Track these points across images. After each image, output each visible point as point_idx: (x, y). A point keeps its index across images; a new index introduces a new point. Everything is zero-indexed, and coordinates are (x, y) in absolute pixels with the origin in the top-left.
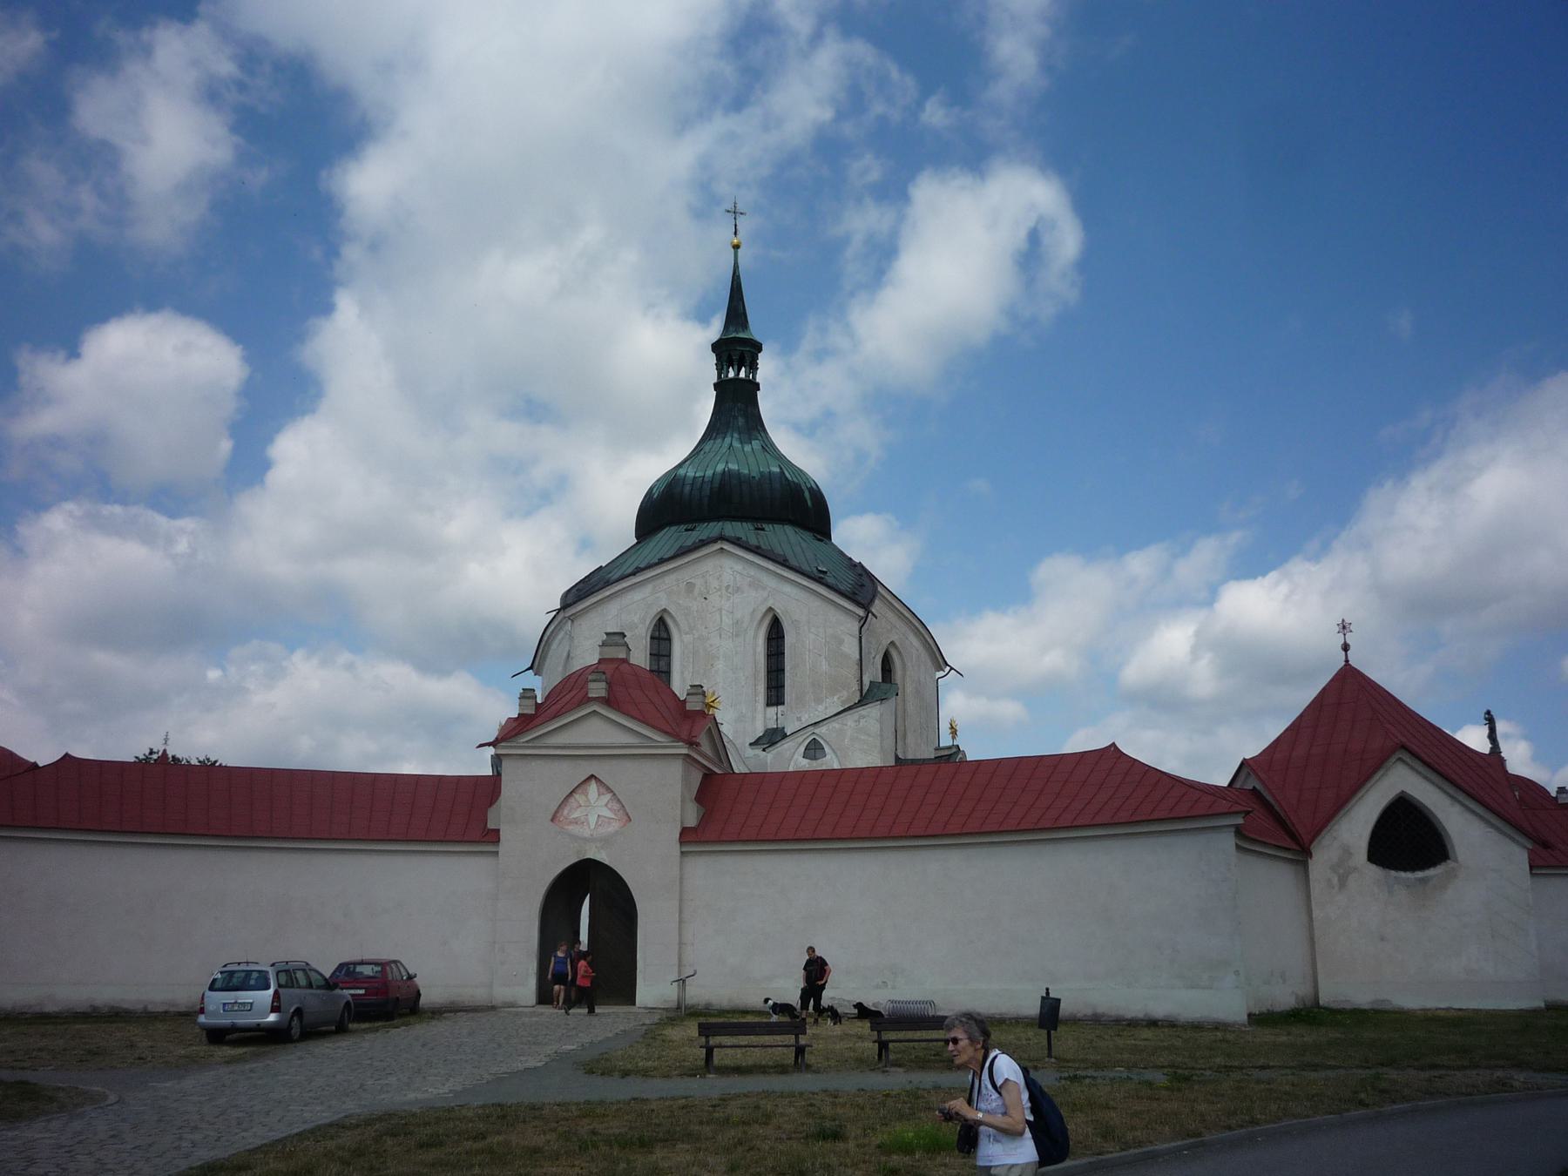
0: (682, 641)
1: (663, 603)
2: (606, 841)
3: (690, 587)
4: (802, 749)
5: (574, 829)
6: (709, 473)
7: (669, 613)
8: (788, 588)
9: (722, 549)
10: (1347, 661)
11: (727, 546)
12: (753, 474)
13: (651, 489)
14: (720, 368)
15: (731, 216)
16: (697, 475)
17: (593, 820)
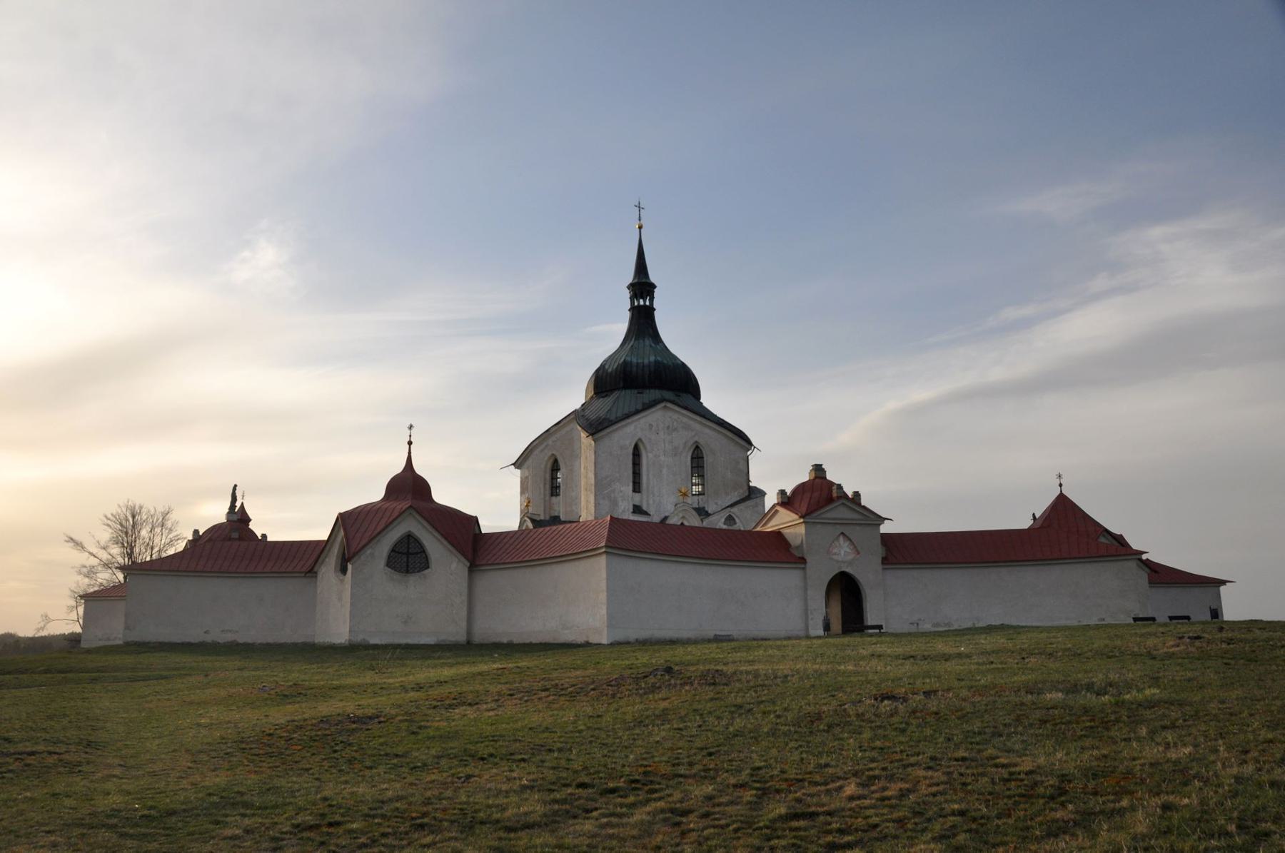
0: (647, 456)
1: (639, 435)
2: (850, 563)
3: (651, 426)
4: (723, 520)
5: (835, 557)
6: (646, 361)
7: (643, 443)
8: (707, 431)
9: (665, 406)
10: (1061, 491)
11: (669, 405)
12: (670, 363)
13: (602, 367)
14: (632, 299)
15: (638, 209)
16: (640, 361)
17: (842, 553)
